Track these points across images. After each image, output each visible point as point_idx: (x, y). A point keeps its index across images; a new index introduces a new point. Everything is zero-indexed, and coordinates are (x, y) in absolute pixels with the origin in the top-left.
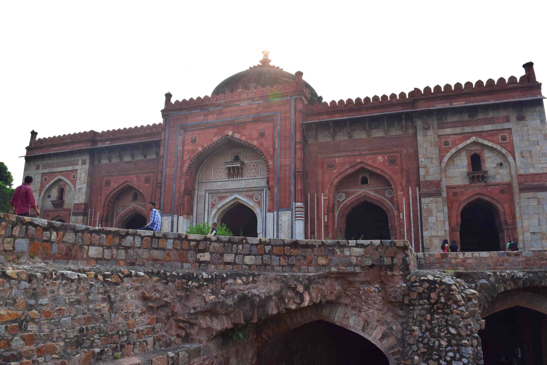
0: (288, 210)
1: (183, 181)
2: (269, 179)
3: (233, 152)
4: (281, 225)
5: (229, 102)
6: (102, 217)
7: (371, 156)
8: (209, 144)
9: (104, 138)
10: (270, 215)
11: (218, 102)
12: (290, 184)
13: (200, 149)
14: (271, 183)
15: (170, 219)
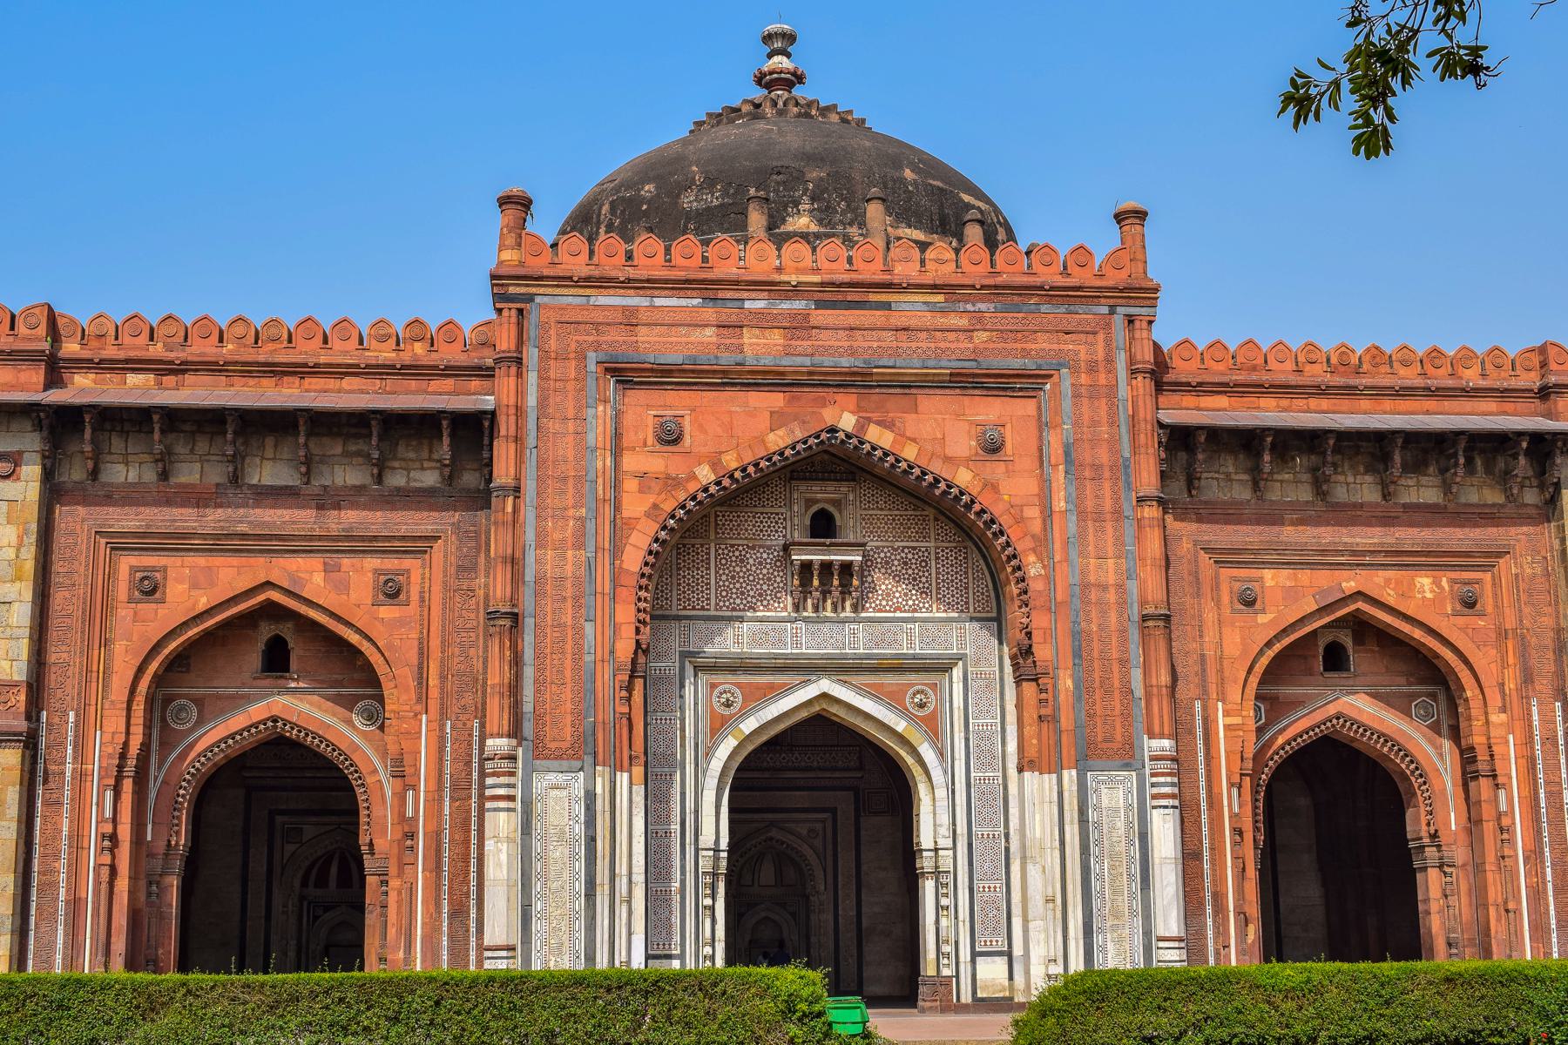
0: (1127, 767)
1: (626, 614)
2: (1029, 635)
3: (827, 498)
4: (1098, 825)
5: (840, 285)
6: (123, 756)
7: (1391, 574)
8: (748, 458)
9: (110, 352)
10: (1038, 785)
11: (794, 279)
12: (1124, 662)
13: (705, 474)
14: (1042, 652)
15: (579, 783)
